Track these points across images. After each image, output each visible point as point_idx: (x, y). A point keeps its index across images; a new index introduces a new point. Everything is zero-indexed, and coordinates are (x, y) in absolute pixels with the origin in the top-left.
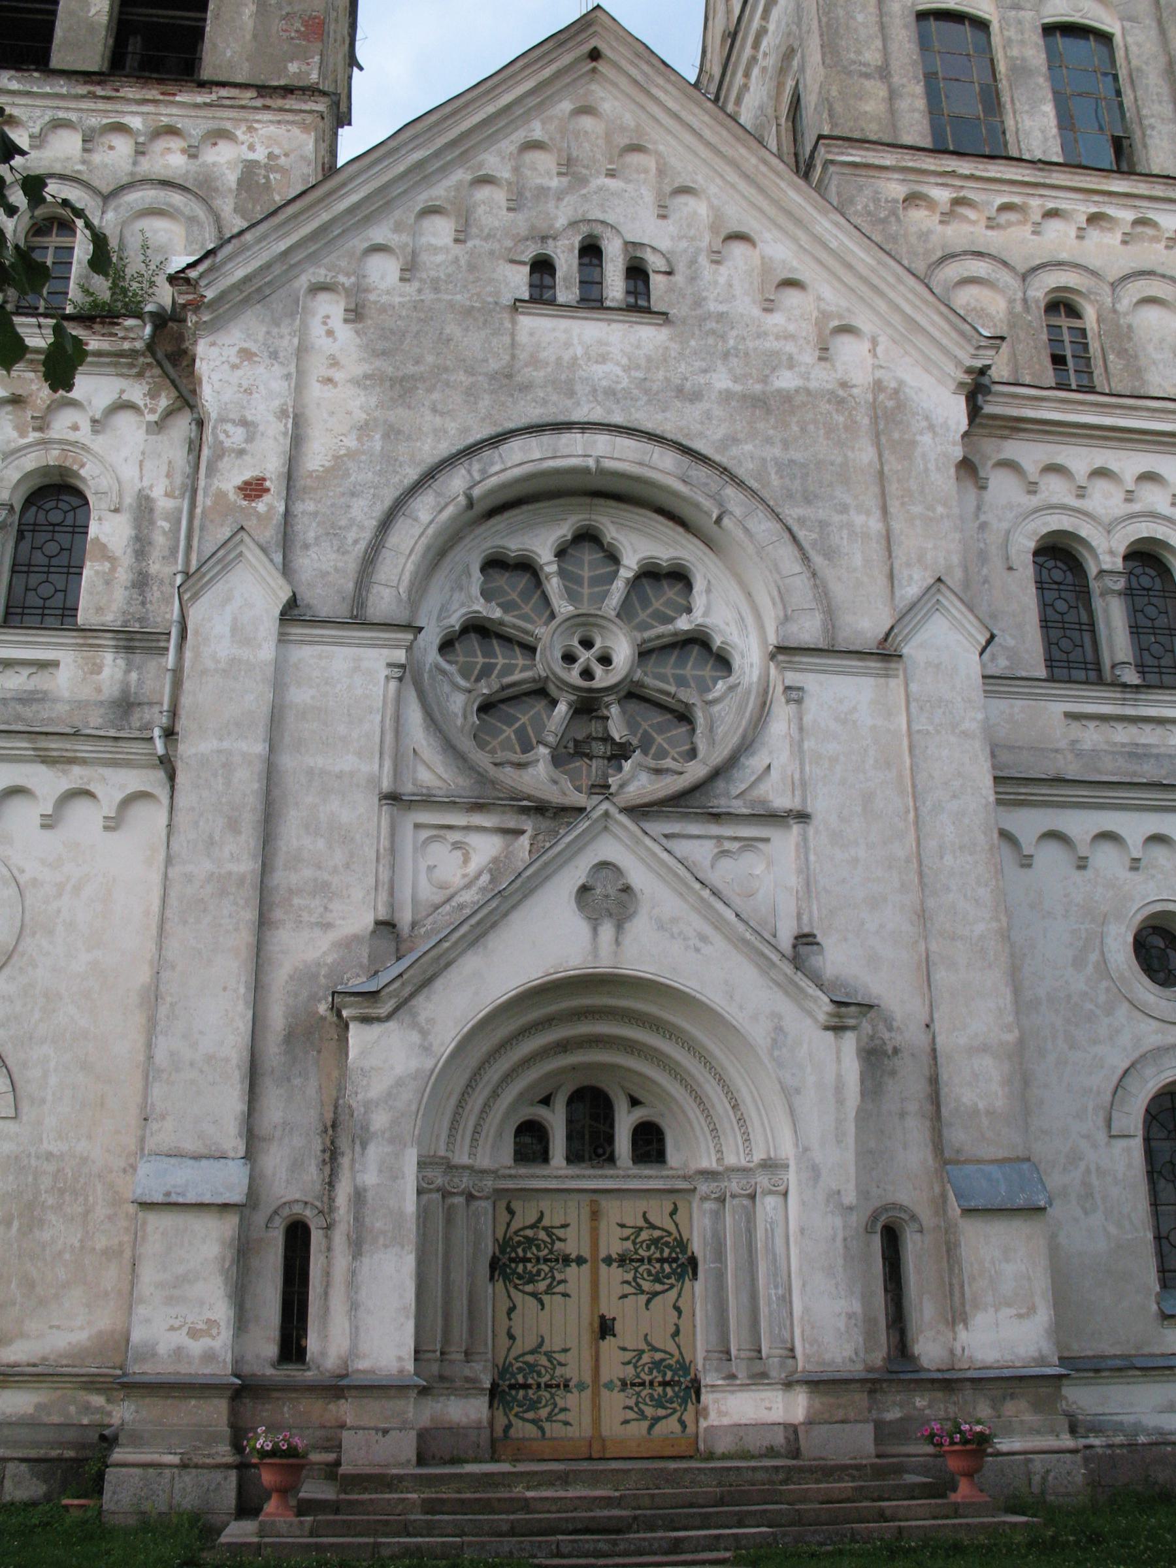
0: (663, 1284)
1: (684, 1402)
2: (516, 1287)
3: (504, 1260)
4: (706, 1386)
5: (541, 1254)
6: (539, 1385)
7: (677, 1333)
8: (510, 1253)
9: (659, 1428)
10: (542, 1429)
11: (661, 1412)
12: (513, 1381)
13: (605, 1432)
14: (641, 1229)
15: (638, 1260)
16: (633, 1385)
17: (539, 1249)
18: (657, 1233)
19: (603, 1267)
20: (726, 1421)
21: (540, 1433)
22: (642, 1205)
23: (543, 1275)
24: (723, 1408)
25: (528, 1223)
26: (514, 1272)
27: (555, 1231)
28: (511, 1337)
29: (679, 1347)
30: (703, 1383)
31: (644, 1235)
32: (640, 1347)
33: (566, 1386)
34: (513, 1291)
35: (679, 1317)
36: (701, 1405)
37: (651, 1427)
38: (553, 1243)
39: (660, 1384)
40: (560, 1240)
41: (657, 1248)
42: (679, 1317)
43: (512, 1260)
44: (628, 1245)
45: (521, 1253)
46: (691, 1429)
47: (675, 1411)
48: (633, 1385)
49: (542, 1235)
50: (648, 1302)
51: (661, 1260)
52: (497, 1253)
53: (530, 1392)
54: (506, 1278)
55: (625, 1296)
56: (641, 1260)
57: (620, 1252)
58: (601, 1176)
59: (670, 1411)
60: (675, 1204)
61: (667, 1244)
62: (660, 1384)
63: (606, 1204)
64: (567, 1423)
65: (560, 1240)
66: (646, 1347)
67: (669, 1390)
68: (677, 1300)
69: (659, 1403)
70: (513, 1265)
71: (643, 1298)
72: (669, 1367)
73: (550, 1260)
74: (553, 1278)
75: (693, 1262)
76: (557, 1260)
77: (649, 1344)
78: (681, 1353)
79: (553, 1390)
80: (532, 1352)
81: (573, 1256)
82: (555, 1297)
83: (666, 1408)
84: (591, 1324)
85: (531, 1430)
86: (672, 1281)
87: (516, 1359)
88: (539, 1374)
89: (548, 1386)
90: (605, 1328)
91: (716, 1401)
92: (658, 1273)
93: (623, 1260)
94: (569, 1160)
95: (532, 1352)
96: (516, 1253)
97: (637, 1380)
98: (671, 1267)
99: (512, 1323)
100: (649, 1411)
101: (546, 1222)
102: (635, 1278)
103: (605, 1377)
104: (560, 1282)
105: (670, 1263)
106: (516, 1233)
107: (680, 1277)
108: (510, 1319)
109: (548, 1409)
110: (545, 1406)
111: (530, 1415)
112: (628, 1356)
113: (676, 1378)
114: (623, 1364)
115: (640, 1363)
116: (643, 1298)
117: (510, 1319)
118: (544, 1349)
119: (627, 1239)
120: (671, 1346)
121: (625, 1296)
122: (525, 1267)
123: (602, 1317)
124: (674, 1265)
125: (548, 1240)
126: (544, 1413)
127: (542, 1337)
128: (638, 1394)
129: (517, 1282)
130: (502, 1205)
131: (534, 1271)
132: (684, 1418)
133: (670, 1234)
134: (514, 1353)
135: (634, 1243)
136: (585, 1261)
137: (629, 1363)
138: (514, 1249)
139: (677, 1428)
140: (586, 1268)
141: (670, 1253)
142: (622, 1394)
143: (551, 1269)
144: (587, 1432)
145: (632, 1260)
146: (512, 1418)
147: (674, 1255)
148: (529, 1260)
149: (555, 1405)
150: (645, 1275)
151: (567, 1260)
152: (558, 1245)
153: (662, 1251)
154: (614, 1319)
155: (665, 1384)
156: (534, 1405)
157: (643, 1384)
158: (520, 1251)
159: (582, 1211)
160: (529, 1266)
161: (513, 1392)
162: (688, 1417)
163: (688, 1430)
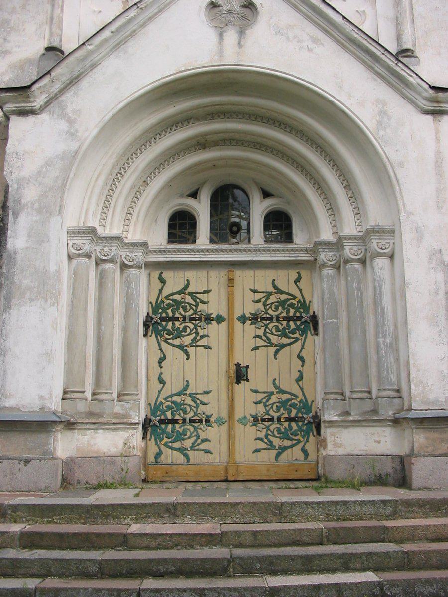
0: (290, 338)
1: (307, 434)
2: (166, 341)
3: (156, 318)
4: (324, 422)
5: (187, 314)
6: (184, 421)
7: (300, 378)
8: (161, 314)
9: (285, 456)
10: (186, 456)
11: (287, 443)
12: (163, 417)
13: (239, 458)
14: (270, 293)
15: (268, 319)
16: (263, 420)
18: (284, 297)
19: (224, 314)
20: (341, 451)
21: (185, 460)
22: (271, 274)
23: (188, 331)
24: (338, 441)
26: (165, 329)
27: (198, 295)
28: (162, 381)
29: (302, 389)
30: (322, 420)
31: (273, 299)
33: (207, 421)
34: (164, 345)
35: (302, 366)
36: (322, 437)
37: (279, 455)
38: (197, 306)
39: (287, 420)
41: (283, 309)
42: (302, 366)
43: (162, 319)
44: (260, 306)
45: (171, 315)
46: (312, 457)
47: (299, 441)
48: (263, 420)
49: (188, 299)
50: (277, 352)
51: (288, 319)
52: (151, 314)
53: (177, 426)
54: (158, 334)
55: (257, 348)
56: (270, 319)
57: (253, 312)
58: (236, 250)
59: (294, 442)
60: (297, 273)
61: (292, 306)
62: (287, 420)
63: (238, 274)
64: (207, 452)
66: (275, 391)
67: (294, 425)
68: (301, 351)
69: (285, 436)
70: (164, 323)
71: (272, 350)
72: (294, 406)
73: (194, 319)
74: (197, 333)
75: (314, 320)
76: (200, 319)
77: (276, 387)
78: (304, 394)
79: (197, 424)
80: (179, 394)
81: (213, 316)
83: (291, 440)
84: (228, 371)
85: (178, 457)
86: (297, 335)
87: (165, 399)
88: (185, 413)
89: (192, 421)
90: (240, 374)
91: (332, 434)
92: (284, 329)
93: (255, 319)
94: (212, 241)
95: (179, 394)
96: (167, 314)
97: (267, 417)
98: (295, 324)
99: (162, 370)
100: (277, 442)
101: (191, 289)
102: (265, 334)
103: (239, 415)
104: (202, 337)
105: (294, 321)
106: (166, 297)
107: (304, 333)
108: (161, 367)
109: (193, 440)
110: (189, 438)
111: (177, 445)
112: (260, 396)
113: (300, 415)
115: (270, 402)
116: (273, 349)
117: (161, 367)
118: (188, 392)
119: (259, 301)
120: (296, 390)
121: (257, 348)
123: (238, 365)
124: (298, 323)
126: (188, 443)
127: (187, 381)
128: (268, 428)
130: (156, 274)
131: (181, 327)
132: (306, 447)
133: (295, 297)
134: (164, 394)
135: (265, 305)
136: (224, 320)
137: (260, 402)
138: (165, 310)
139: (301, 456)
140: (224, 325)
141: (295, 313)
143: (195, 327)
144: (224, 459)
145: (263, 319)
146: (162, 447)
147: (298, 314)
148: (177, 319)
149: (198, 437)
150: (274, 331)
151: (208, 319)
152: (201, 307)
153: (288, 312)
154: (248, 367)
155: (290, 420)
156: (180, 437)
157: (272, 420)
158: (169, 312)
159: (221, 279)
160: (177, 324)
161: (163, 426)
162: (310, 447)
163: (309, 458)
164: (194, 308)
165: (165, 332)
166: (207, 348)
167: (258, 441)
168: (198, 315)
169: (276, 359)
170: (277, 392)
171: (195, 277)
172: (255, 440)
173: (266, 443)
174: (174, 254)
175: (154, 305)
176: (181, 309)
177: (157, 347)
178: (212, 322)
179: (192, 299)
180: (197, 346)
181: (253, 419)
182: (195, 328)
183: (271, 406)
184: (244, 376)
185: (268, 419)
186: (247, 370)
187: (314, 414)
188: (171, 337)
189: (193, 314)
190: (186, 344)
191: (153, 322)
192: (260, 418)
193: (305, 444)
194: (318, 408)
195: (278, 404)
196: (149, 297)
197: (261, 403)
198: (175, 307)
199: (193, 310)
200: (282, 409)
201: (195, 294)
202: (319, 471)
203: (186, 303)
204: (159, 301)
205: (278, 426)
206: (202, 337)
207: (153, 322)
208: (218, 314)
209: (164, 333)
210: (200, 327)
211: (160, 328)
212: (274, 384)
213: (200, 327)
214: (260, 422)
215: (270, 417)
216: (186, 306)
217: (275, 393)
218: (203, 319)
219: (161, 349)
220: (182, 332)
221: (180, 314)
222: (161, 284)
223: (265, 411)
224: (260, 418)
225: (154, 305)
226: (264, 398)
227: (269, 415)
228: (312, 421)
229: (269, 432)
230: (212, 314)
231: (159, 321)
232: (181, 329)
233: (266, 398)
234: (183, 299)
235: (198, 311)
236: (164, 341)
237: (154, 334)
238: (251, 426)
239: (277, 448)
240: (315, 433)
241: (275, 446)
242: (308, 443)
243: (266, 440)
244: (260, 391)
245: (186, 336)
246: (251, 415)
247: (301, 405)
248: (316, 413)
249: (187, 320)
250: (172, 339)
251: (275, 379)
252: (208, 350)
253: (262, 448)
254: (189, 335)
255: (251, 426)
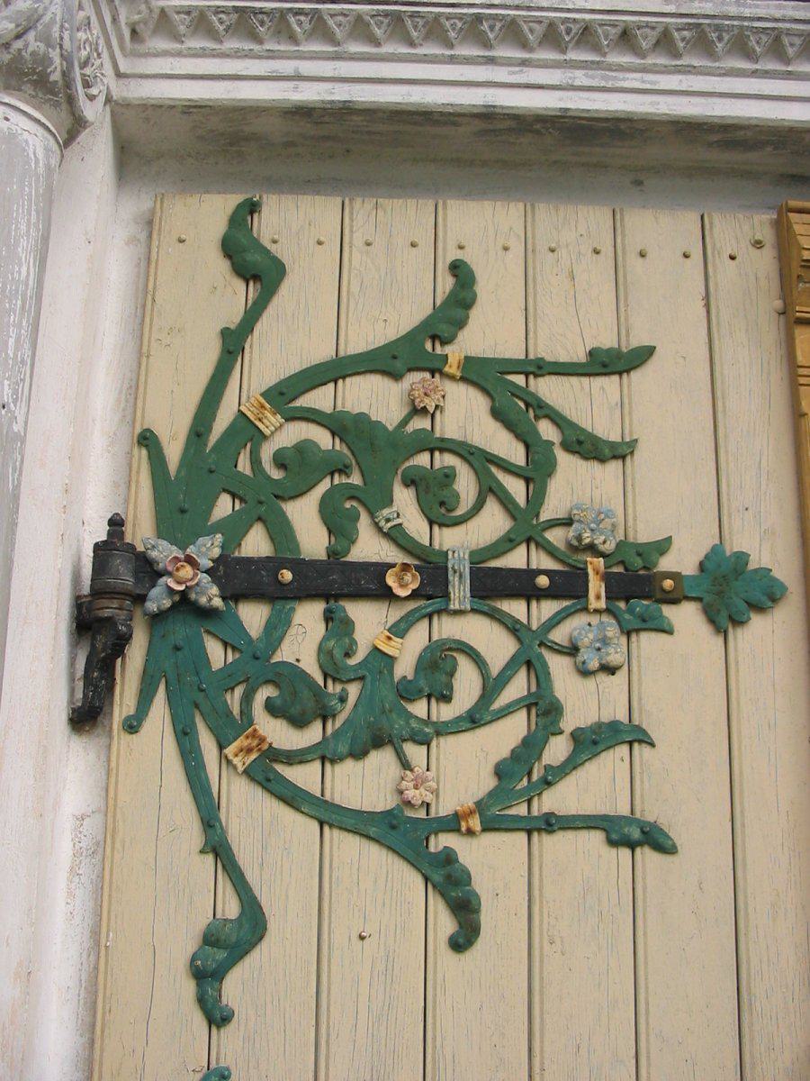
5: (458, 542)
8: (234, 530)
17: (440, 510)
23: (467, 685)
25: (364, 337)
38: (537, 472)
40: (588, 447)
45: (313, 540)
52: (142, 532)
65: (588, 447)
70: (253, 616)
73: (522, 585)
74: (544, 708)
76: (569, 586)
81: (682, 560)
82: (555, 845)
96: (281, 532)
99: (230, 1045)
104: (591, 742)
106: (283, 396)
108: (217, 1017)
117: (217, 1017)
122: (338, 625)
125: (509, 448)
129: (279, 734)
131: (407, 654)
136: (765, 596)
148: (371, 583)
159: (725, 273)
160: (369, 620)
164: (516, 488)
165: (265, 693)
166: (632, 846)
168: (551, 551)
171: (517, 249)
174: (355, 48)
175: (173, 452)
176: (404, 499)
177: (194, 835)
178: (668, 611)
179: (496, 414)
180: (551, 824)
182: (528, 661)
188: (313, 734)
189: (507, 543)
190: (444, 808)
191: (158, 599)
196: (134, 390)
198: (356, 479)
199: (506, 502)
201: (519, 380)
203: (445, 446)
204: (224, 419)
206: (591, 742)
207: (158, 599)
208: (716, 551)
209: (247, 699)
210: (572, 650)
211: (217, 654)
213: (572, 650)
216: (449, 476)
218: (596, 586)
219: (218, 848)
220: (407, 692)
221: (396, 536)
222: (237, 296)
225: (173, 452)
230: (663, 546)
231: (211, 595)
232: (405, 668)
234: (418, 411)
235: (545, 516)
236: (248, 773)
237: (159, 707)
245: (443, 730)
249: (460, 592)
250: (325, 755)
252: (646, 855)
254: (473, 720)
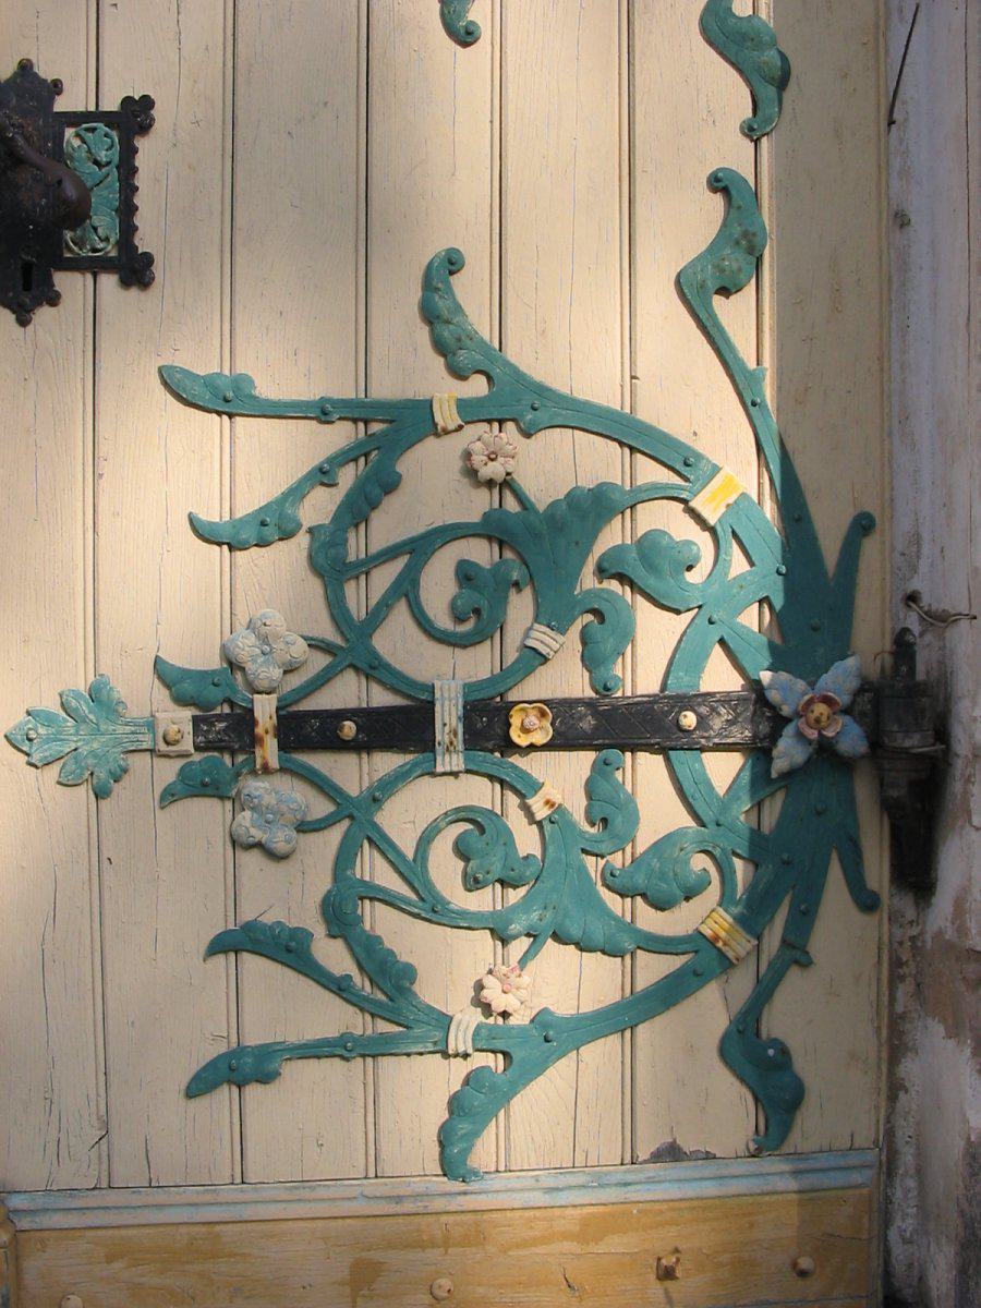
32: (386, 388)
66: (446, 393)
67: (646, 774)
97: (348, 692)
114: (204, 533)
115: (390, 525)
132: (778, 1022)
137: (270, 526)
142: (208, 815)
154: (135, 117)
163: (811, 1127)
167: (253, 964)
169: (465, 37)
170: (471, 412)
172: (221, 946)
173: (339, 987)
181: (187, 714)
183: (399, 564)
184: (77, 214)
185: (365, 716)
186: (129, 152)
187: (874, 672)
192: (265, 711)
193: (764, 992)
194: (912, 598)
195: (481, 553)
197: (286, 536)
200: (520, 608)
202: (899, 1251)
205: (479, 793)
212: (430, 315)
214: (269, 750)
215: (381, 698)
217: (446, 416)
223: (327, 631)
224: (265, 711)
226: (323, 475)
227: (374, 669)
228: (850, 738)
229: (374, 869)
233: (347, 477)
238: (169, 797)
239: (459, 1040)
240: (877, 868)
241: (444, 1022)
242: (794, 977)
243: (334, 956)
244: (267, 388)
246: (161, 669)
247: (738, 564)
248: (903, 648)
251: (452, 263)
253: (293, 1038)
255: (169, 797)
